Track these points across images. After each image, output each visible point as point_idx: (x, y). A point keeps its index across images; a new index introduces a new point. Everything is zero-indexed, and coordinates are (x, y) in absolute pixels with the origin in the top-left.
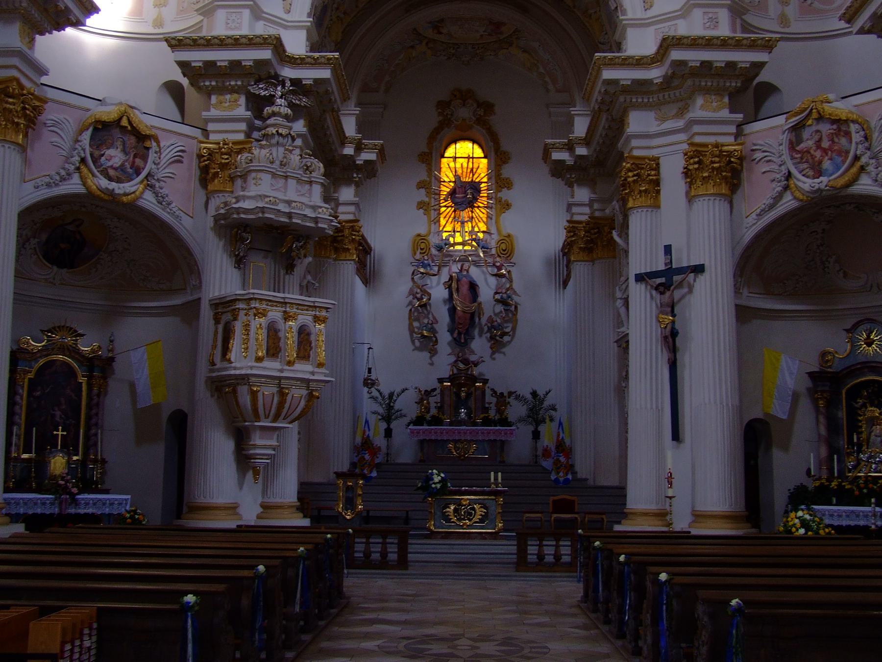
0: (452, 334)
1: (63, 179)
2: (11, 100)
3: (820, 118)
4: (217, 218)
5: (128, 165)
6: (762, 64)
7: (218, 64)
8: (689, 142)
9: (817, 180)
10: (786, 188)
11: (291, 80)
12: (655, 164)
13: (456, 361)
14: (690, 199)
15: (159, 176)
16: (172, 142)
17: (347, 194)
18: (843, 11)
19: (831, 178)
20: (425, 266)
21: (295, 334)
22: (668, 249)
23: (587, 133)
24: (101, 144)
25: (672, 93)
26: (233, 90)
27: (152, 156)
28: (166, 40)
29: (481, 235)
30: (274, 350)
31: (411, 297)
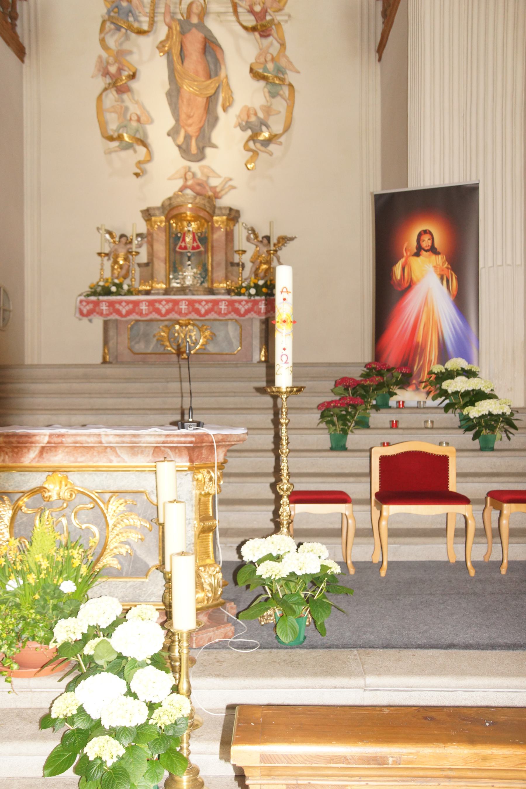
0: (174, 140)
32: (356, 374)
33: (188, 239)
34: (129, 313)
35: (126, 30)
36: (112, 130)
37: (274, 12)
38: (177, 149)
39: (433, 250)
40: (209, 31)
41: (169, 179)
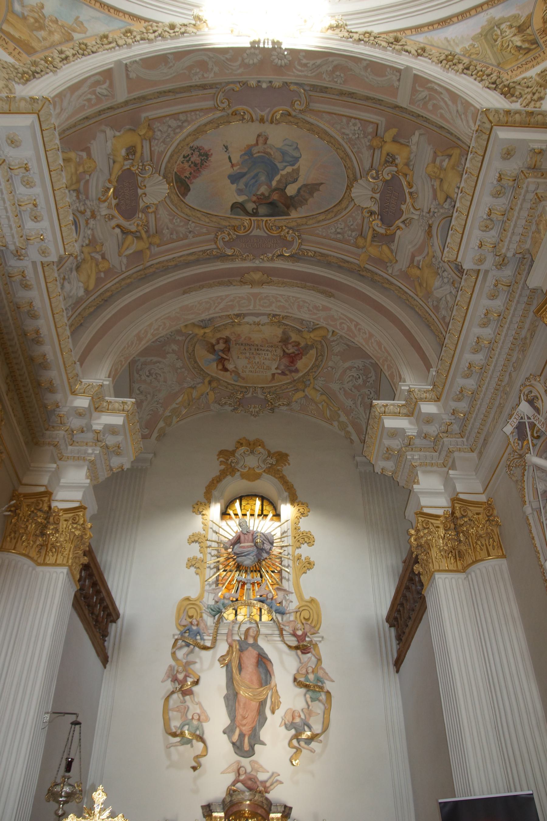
0: (230, 737)
13: (234, 784)
35: (194, 646)
36: (175, 727)
37: (311, 634)
38: (231, 745)
40: (262, 649)
41: (222, 773)
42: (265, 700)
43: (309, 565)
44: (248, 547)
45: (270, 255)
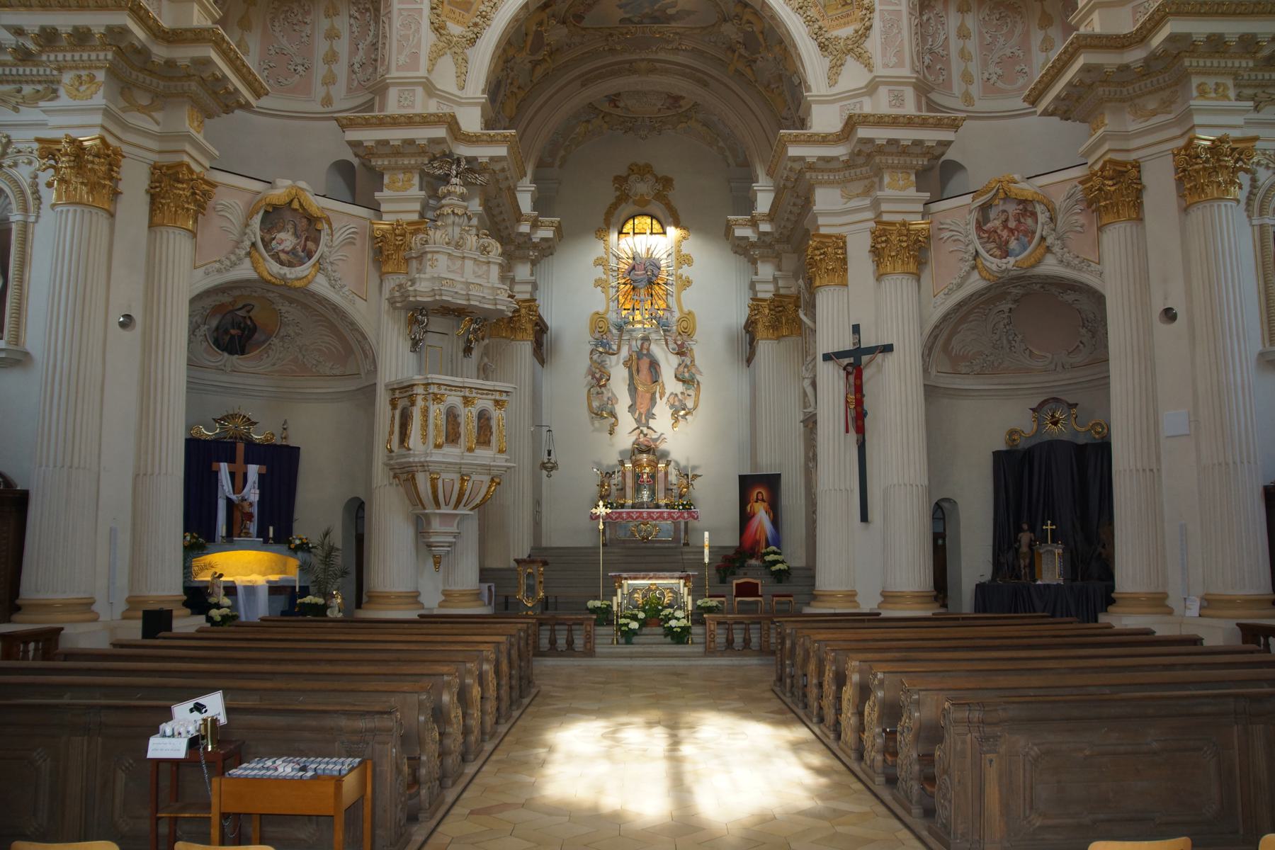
1: (234, 265)
2: (180, 186)
3: (1007, 198)
4: (392, 302)
5: (299, 249)
6: (948, 144)
7: (391, 143)
8: (876, 220)
9: (1004, 261)
10: (974, 267)
11: (466, 158)
12: (840, 242)
14: (879, 277)
15: (331, 259)
16: (344, 224)
17: (523, 271)
18: (1027, 92)
19: (1018, 258)
20: (603, 345)
21: (475, 419)
22: (856, 329)
23: (770, 210)
24: (272, 228)
25: (858, 171)
26: (407, 170)
27: (324, 238)
28: (336, 119)
29: (661, 313)
30: (453, 436)
31: (590, 377)
32: (731, 553)
33: (645, 476)
34: (616, 518)
39: (763, 500)
42: (655, 392)
43: (688, 283)
44: (641, 275)
45: (654, 49)
